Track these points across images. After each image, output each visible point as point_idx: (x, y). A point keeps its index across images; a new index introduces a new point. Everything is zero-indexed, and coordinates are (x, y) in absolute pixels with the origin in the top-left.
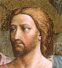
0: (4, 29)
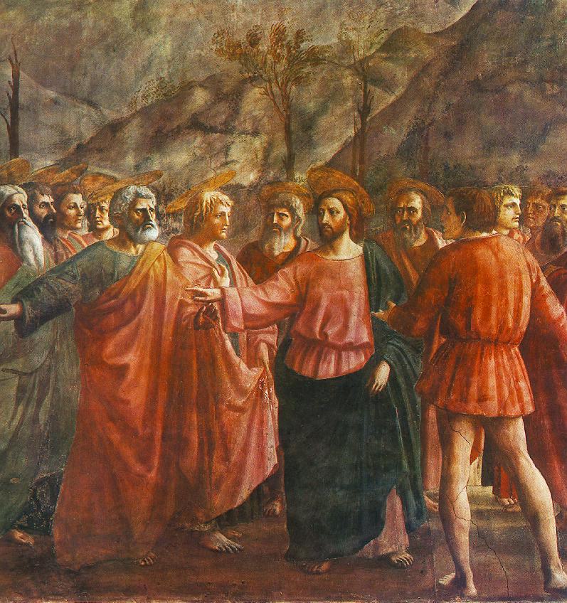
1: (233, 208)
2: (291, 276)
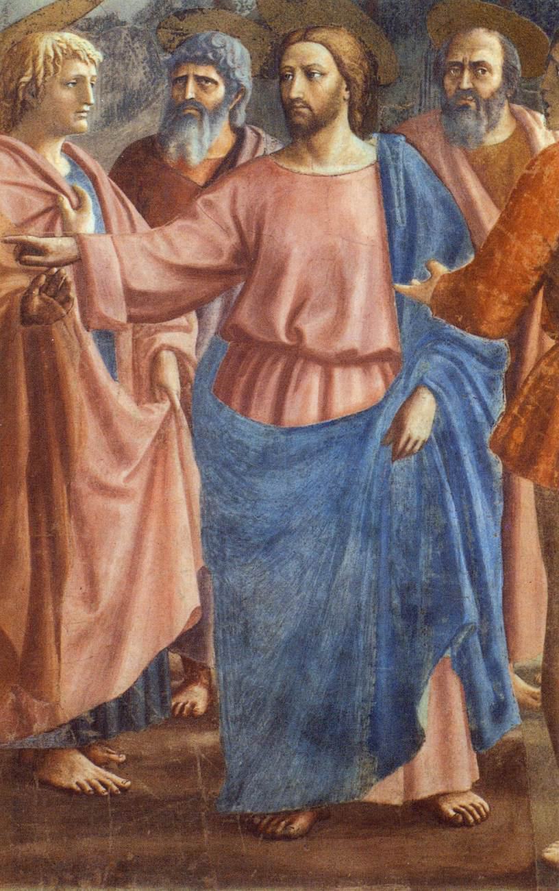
0: (267, 75)
1: (101, 68)
2: (224, 206)
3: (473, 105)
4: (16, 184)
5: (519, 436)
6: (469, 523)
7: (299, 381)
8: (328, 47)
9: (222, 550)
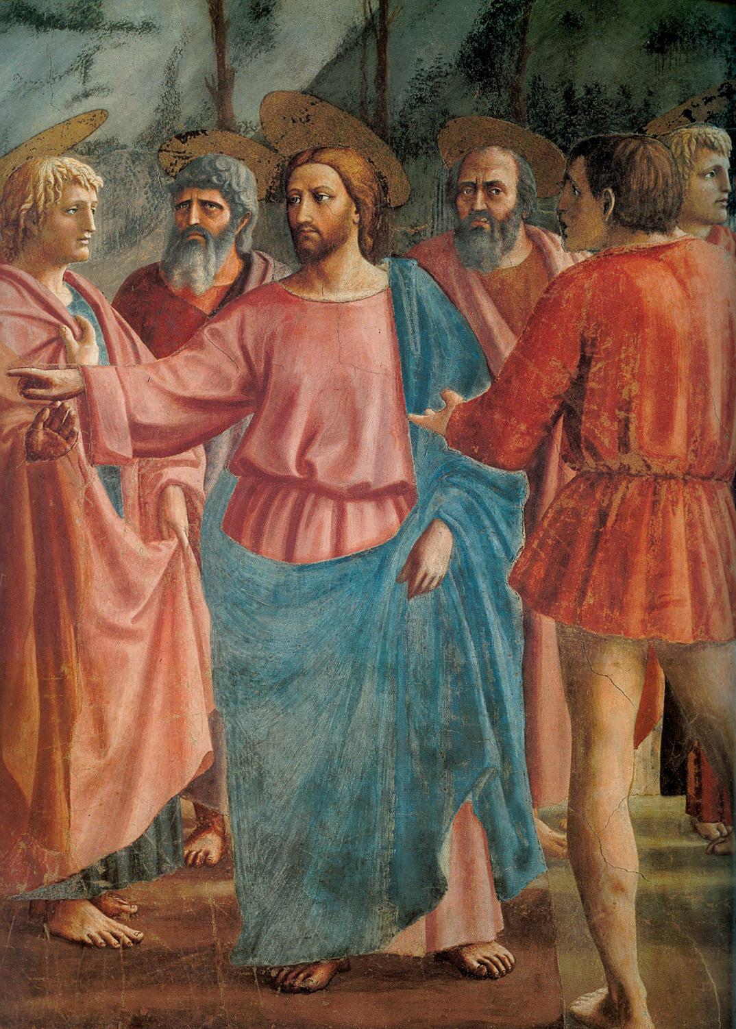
1: (101, 193)
2: (232, 337)
3: (487, 226)
4: (20, 315)
5: (539, 571)
6: (489, 665)
7: (311, 514)
8: (336, 168)
9: (234, 693)
